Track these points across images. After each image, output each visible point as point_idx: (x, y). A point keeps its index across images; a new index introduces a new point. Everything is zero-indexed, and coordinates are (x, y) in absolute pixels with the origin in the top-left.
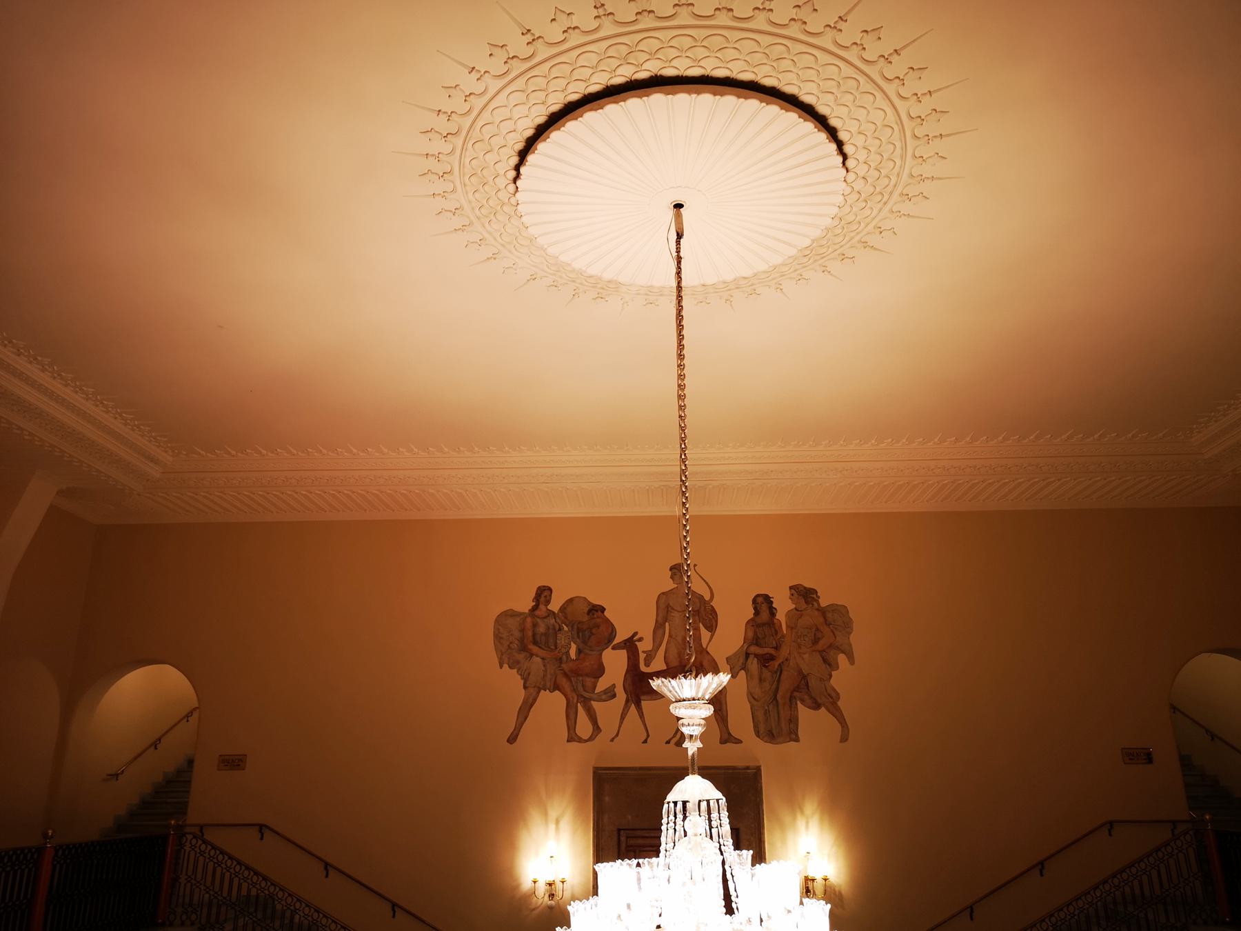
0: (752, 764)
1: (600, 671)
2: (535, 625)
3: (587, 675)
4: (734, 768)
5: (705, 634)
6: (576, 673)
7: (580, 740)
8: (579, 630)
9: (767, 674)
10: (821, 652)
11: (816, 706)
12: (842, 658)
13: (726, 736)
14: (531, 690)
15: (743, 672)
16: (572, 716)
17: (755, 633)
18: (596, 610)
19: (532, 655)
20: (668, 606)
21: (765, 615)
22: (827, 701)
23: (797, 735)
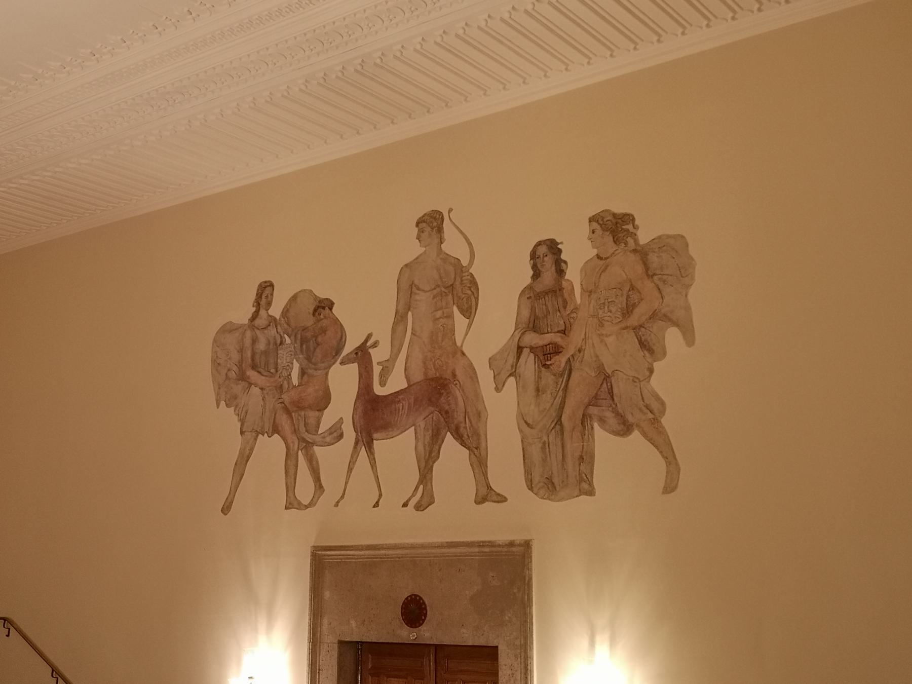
0: (518, 537)
1: (324, 400)
2: (254, 341)
3: (310, 407)
4: (491, 544)
5: (460, 321)
6: (299, 405)
7: (300, 506)
8: (304, 341)
9: (548, 378)
10: (636, 329)
11: (625, 428)
12: (672, 337)
13: (483, 491)
14: (249, 435)
15: (512, 380)
16: (292, 472)
17: (533, 309)
18: (324, 306)
19: (250, 384)
20: (411, 285)
21: (548, 277)
22: (640, 418)
23: (591, 484)
